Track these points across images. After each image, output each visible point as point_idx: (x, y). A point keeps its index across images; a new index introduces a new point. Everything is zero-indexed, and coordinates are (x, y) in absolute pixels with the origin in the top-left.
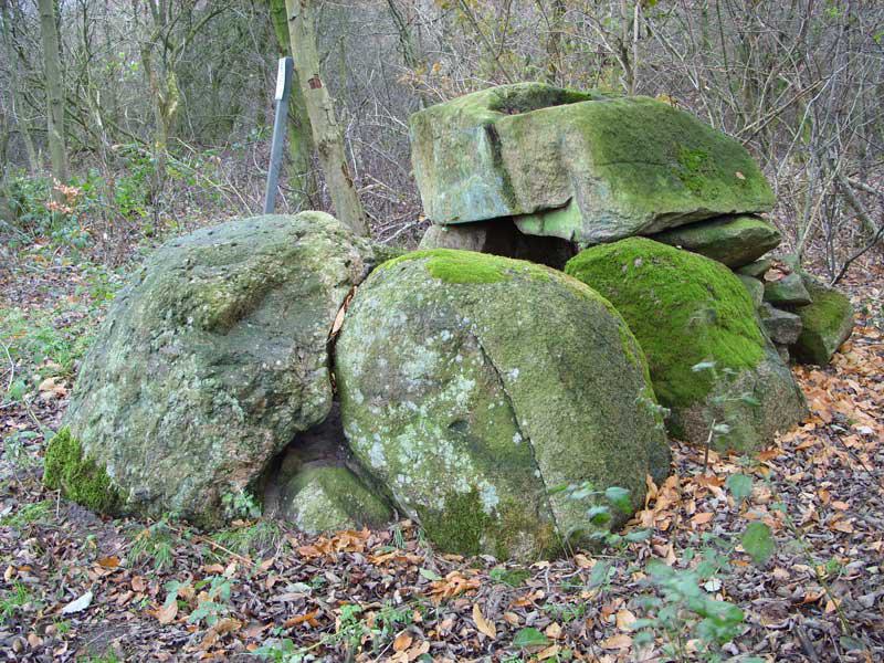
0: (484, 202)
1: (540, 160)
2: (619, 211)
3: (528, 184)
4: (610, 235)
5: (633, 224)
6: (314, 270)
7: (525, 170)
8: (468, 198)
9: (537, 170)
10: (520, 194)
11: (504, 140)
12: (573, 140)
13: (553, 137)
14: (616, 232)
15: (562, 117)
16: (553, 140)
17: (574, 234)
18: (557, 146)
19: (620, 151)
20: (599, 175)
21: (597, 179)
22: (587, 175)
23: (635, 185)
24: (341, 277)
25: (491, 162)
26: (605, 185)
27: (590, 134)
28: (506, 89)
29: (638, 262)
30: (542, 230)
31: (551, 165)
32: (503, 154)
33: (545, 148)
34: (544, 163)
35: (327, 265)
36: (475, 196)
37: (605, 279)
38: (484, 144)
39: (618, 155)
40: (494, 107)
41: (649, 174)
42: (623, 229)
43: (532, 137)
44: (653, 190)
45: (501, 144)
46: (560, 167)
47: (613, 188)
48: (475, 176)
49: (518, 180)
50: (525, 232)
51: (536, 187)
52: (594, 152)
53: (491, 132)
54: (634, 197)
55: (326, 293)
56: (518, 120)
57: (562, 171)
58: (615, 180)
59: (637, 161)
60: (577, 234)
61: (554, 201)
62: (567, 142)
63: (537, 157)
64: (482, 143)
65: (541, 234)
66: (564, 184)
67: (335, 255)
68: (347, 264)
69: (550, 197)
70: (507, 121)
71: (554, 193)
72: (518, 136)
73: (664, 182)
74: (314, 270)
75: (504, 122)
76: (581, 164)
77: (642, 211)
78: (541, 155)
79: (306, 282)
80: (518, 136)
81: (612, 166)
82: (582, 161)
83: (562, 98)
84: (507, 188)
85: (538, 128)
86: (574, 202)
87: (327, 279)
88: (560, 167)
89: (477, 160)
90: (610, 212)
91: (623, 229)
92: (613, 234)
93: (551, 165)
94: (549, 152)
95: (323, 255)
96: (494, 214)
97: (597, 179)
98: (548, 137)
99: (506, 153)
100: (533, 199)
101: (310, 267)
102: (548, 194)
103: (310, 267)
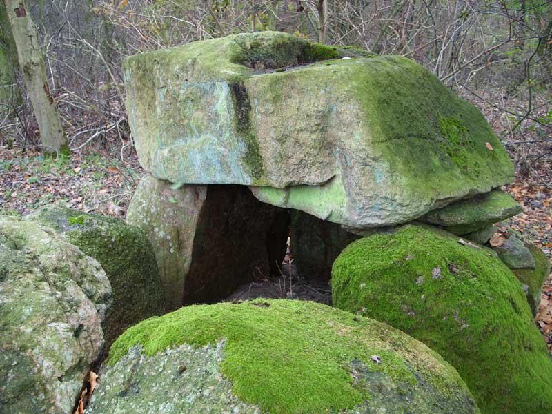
0: (218, 166)
1: (301, 130)
2: (397, 197)
3: (283, 157)
4: (380, 222)
5: (409, 212)
6: (23, 348)
7: (282, 140)
8: (198, 159)
9: (296, 142)
10: (270, 165)
11: (254, 102)
12: (349, 111)
13: (321, 105)
14: (388, 219)
15: (335, 82)
16: (321, 108)
17: (331, 215)
18: (324, 116)
19: (394, 124)
20: (377, 155)
21: (375, 159)
22: (363, 154)
23: (413, 166)
24: (69, 358)
25: (233, 125)
26: (384, 166)
27: (367, 104)
28: (249, 37)
29: (436, 272)
30: (286, 202)
31: (314, 136)
32: (252, 119)
33: (308, 116)
34: (305, 135)
35: (45, 340)
36: (207, 159)
37: (398, 294)
38: (225, 102)
39: (393, 129)
40: (237, 60)
41: (423, 150)
42: (397, 217)
43: (293, 103)
44: (429, 172)
45: (248, 105)
46: (324, 139)
47: (392, 170)
48: (209, 135)
49: (269, 150)
50: (260, 200)
51: (291, 161)
52: (371, 125)
53: (238, 92)
54: (414, 182)
55: (45, 391)
56: (277, 81)
57: (327, 145)
58: (394, 162)
59: (410, 135)
60: (334, 215)
61: (313, 177)
62: (338, 113)
63: (298, 127)
64: (222, 100)
65: (284, 207)
66: (327, 160)
67: (58, 319)
68: (77, 332)
69: (309, 174)
70: (262, 80)
71: (314, 169)
72: (276, 100)
73: (436, 161)
74: (23, 348)
75: (258, 82)
76: (356, 138)
77: (421, 198)
78: (303, 125)
79: (11, 375)
80: (276, 100)
81: (388, 144)
82: (357, 137)
83: (307, 55)
84: (253, 156)
85: (301, 92)
86: (338, 181)
87: (47, 366)
88: (324, 139)
89: (213, 118)
90: (386, 198)
91: (397, 217)
92: (384, 222)
93: (314, 136)
94: (314, 121)
95: (38, 320)
96: (229, 180)
97: (375, 159)
98: (314, 104)
99: (256, 117)
100: (287, 174)
101: (16, 344)
102: (307, 170)
103: (16, 344)
